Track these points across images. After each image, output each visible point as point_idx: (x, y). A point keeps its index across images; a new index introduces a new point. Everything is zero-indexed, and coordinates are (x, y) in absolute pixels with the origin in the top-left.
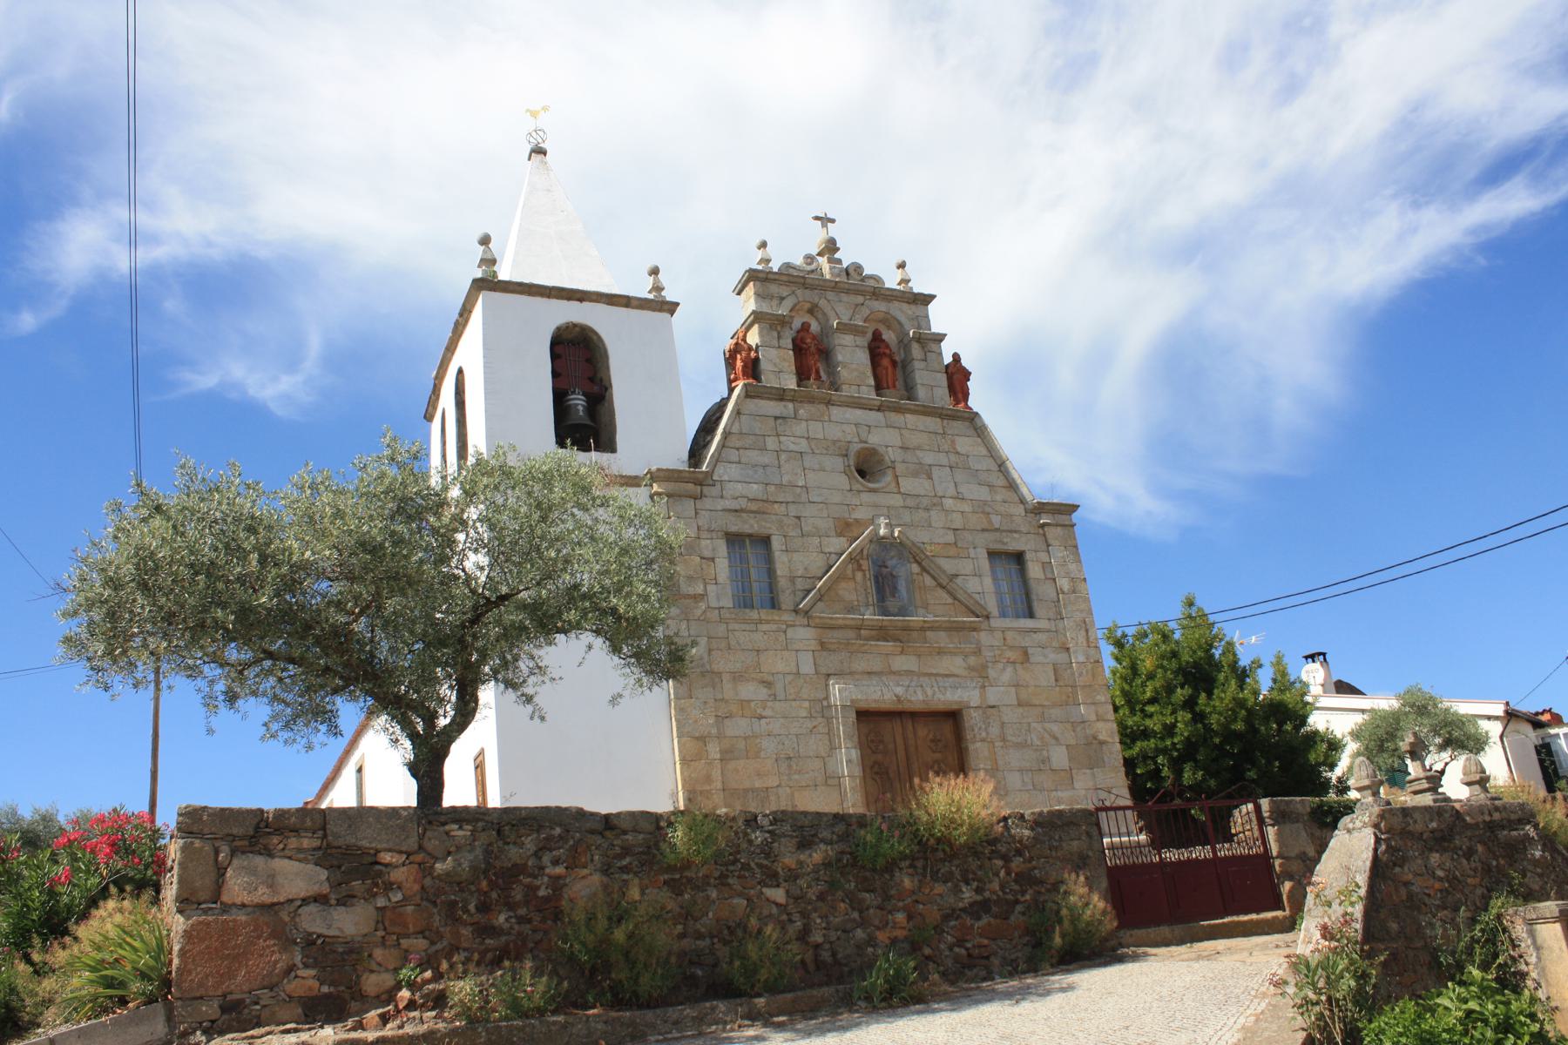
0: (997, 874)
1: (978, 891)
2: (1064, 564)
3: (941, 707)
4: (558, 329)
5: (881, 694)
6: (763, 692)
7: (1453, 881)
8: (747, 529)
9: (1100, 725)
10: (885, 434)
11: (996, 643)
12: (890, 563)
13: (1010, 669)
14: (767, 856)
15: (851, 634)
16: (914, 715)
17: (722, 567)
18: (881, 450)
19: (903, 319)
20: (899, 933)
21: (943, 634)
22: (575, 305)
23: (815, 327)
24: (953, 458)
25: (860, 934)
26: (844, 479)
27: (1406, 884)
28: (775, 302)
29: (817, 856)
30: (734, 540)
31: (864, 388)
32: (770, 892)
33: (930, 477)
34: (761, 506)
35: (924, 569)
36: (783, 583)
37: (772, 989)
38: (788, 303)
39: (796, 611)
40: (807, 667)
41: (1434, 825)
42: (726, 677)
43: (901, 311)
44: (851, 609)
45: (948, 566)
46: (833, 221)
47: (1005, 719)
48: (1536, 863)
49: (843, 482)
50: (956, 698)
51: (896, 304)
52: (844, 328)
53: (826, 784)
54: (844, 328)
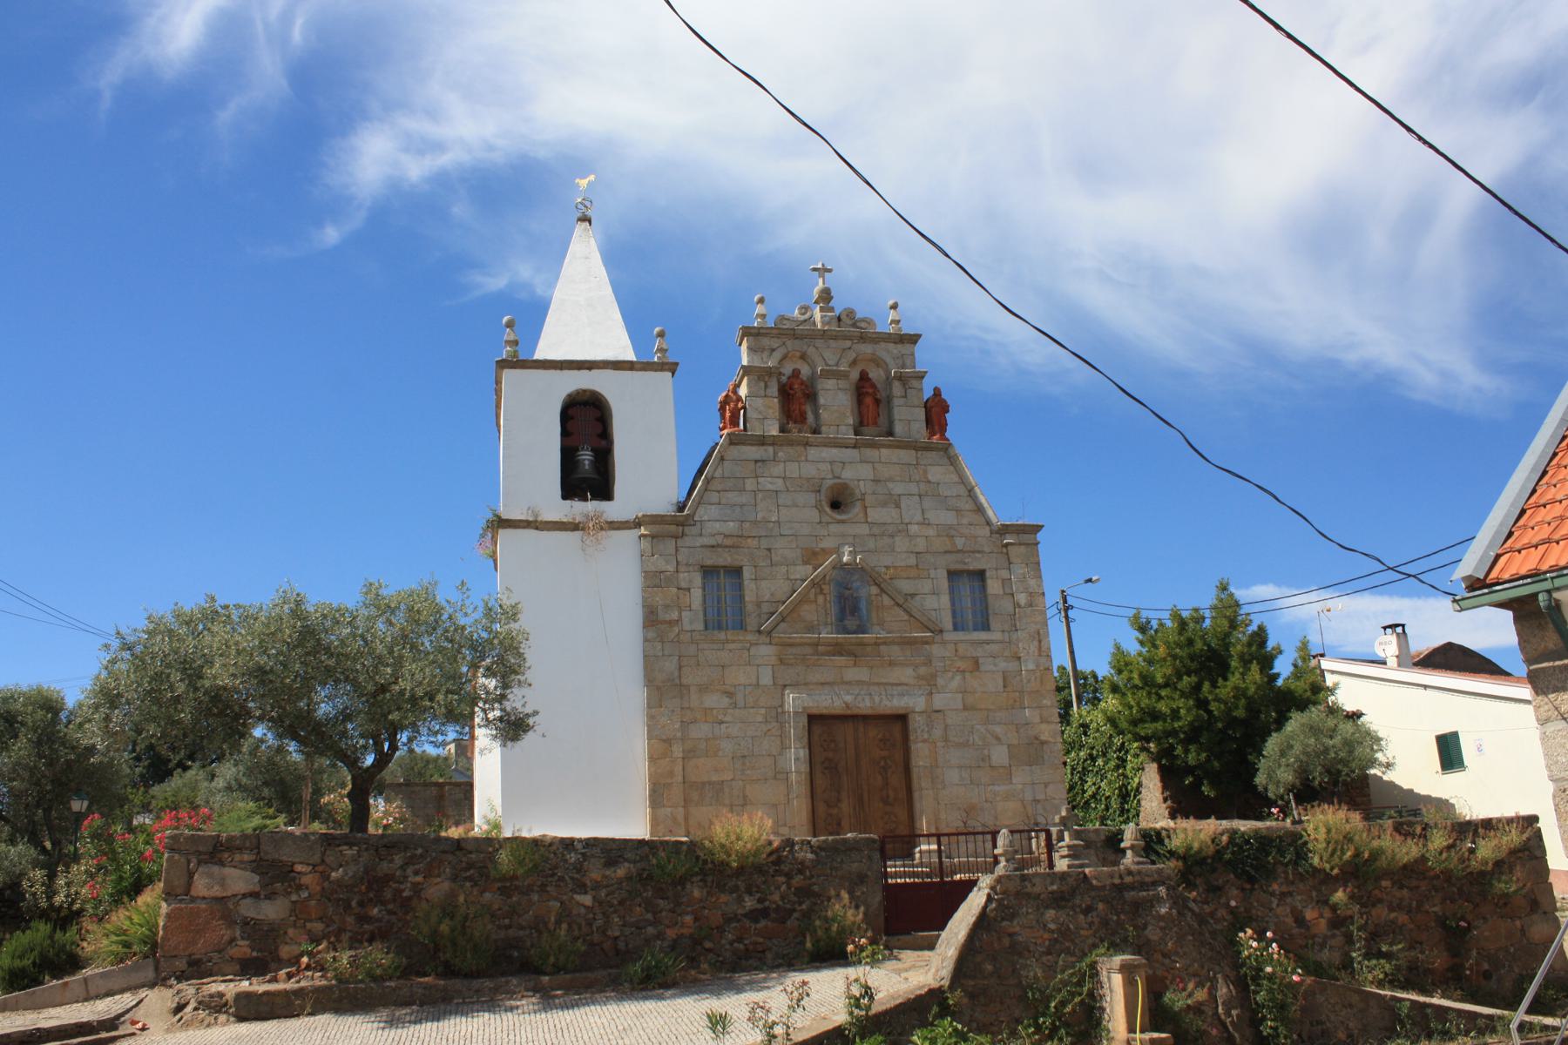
0: (778, 888)
1: (760, 901)
2: (1023, 580)
3: (889, 712)
4: (569, 396)
5: (830, 702)
6: (726, 701)
7: (1064, 932)
8: (721, 562)
9: (1043, 726)
10: (857, 470)
12: (855, 585)
13: (958, 678)
14: (579, 871)
15: (808, 650)
16: (865, 718)
17: (697, 593)
18: (852, 484)
19: (888, 360)
20: (685, 931)
21: (896, 648)
23: (805, 371)
24: (922, 486)
25: (650, 930)
26: (815, 513)
27: (1011, 935)
28: (766, 354)
29: (621, 872)
30: (708, 572)
31: (843, 428)
32: (578, 897)
33: (898, 506)
34: (734, 542)
35: (882, 590)
36: (750, 607)
37: (558, 969)
38: (777, 355)
39: (759, 632)
40: (766, 679)
41: (1055, 887)
43: (887, 352)
44: (810, 629)
45: (905, 586)
46: (830, 271)
47: (949, 721)
48: (1161, 918)
49: (814, 515)
51: (883, 345)
52: (827, 374)
53: (775, 778)
54: (827, 374)
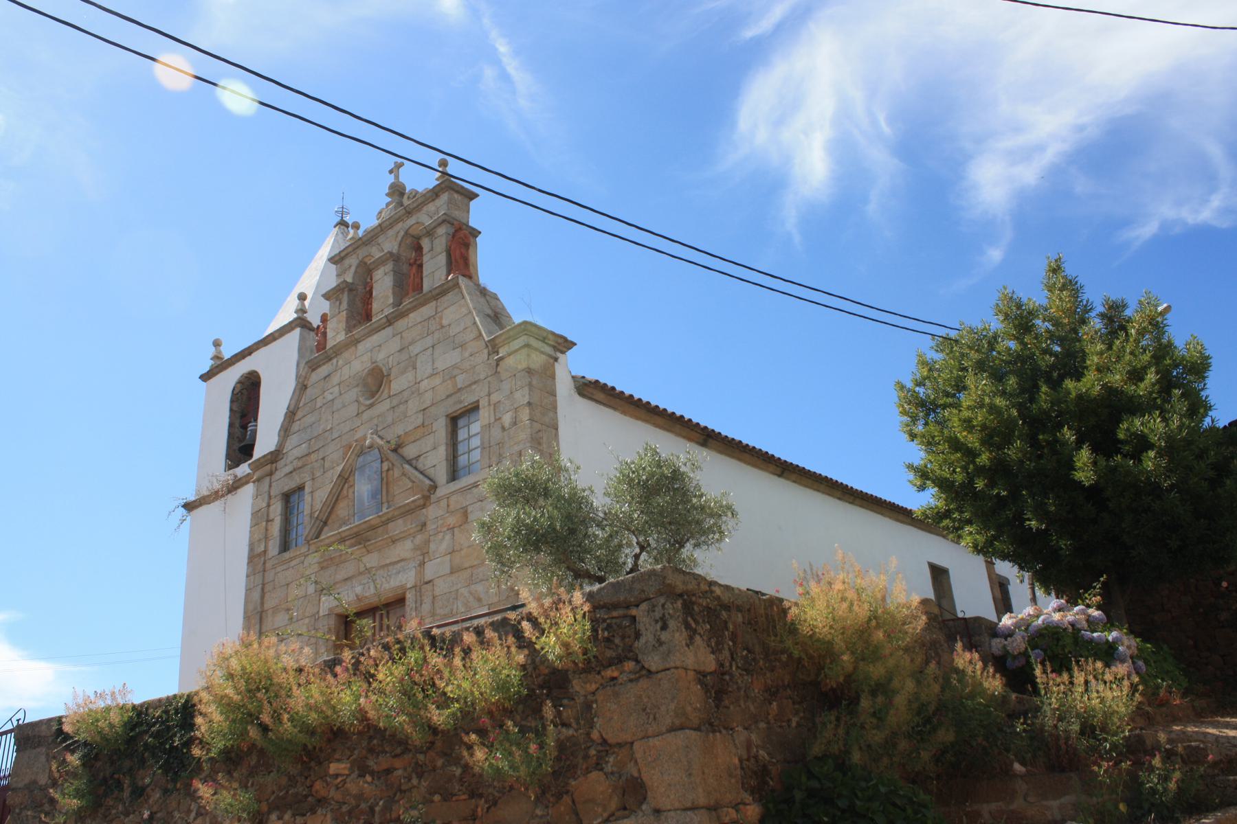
11: (441, 513)
21: (400, 521)
22: (248, 358)
42: (270, 612)
47: (438, 592)
50: (398, 584)
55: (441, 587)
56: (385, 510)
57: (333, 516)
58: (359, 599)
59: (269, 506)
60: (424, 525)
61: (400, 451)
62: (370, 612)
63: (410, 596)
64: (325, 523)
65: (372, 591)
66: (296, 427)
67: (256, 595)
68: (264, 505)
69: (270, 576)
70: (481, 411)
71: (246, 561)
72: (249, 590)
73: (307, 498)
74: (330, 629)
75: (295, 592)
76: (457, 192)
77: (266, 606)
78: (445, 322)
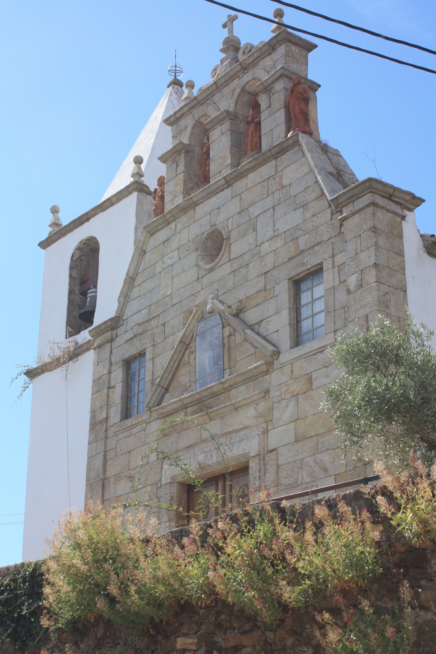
11: (285, 379)
21: (243, 388)
22: (86, 224)
47: (282, 461)
50: (241, 452)
55: (285, 456)
56: (227, 377)
57: (175, 383)
58: (201, 467)
59: (110, 372)
60: (267, 392)
61: (242, 315)
62: (215, 480)
63: (253, 465)
64: (167, 390)
65: (215, 460)
66: (135, 292)
67: (98, 462)
68: (106, 372)
69: (112, 443)
70: (325, 274)
71: (88, 428)
72: (91, 457)
73: (149, 364)
74: (172, 497)
75: (137, 460)
76: (295, 44)
77: (109, 473)
78: (285, 182)
